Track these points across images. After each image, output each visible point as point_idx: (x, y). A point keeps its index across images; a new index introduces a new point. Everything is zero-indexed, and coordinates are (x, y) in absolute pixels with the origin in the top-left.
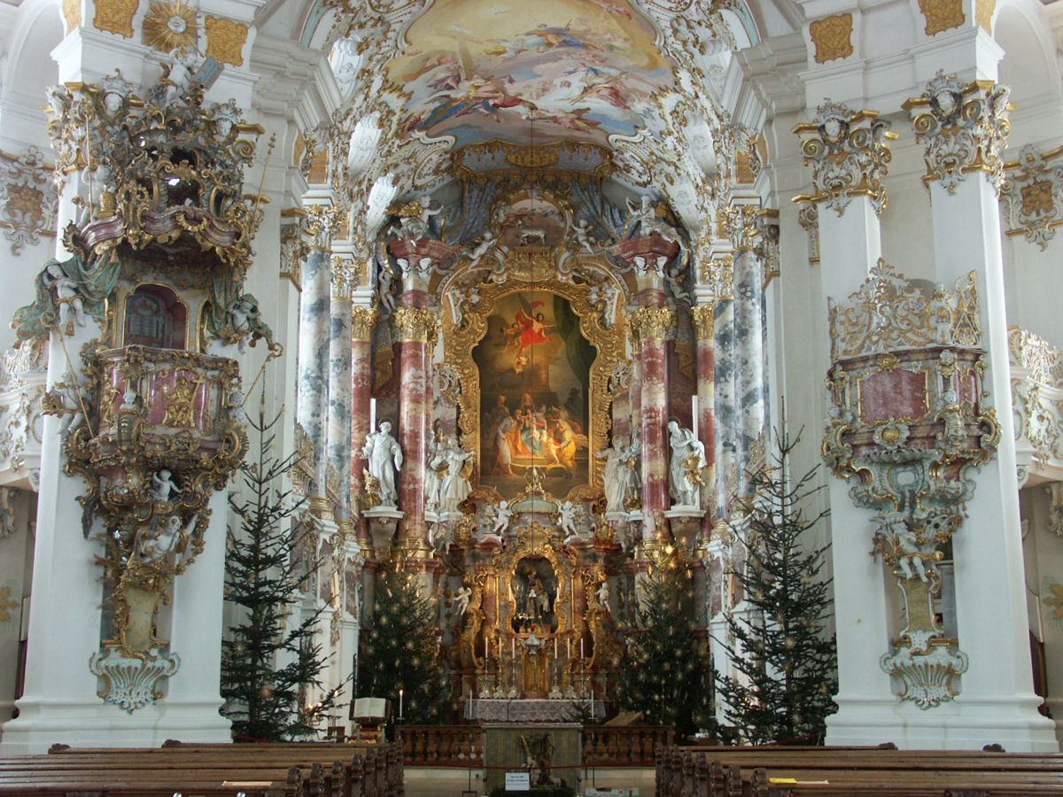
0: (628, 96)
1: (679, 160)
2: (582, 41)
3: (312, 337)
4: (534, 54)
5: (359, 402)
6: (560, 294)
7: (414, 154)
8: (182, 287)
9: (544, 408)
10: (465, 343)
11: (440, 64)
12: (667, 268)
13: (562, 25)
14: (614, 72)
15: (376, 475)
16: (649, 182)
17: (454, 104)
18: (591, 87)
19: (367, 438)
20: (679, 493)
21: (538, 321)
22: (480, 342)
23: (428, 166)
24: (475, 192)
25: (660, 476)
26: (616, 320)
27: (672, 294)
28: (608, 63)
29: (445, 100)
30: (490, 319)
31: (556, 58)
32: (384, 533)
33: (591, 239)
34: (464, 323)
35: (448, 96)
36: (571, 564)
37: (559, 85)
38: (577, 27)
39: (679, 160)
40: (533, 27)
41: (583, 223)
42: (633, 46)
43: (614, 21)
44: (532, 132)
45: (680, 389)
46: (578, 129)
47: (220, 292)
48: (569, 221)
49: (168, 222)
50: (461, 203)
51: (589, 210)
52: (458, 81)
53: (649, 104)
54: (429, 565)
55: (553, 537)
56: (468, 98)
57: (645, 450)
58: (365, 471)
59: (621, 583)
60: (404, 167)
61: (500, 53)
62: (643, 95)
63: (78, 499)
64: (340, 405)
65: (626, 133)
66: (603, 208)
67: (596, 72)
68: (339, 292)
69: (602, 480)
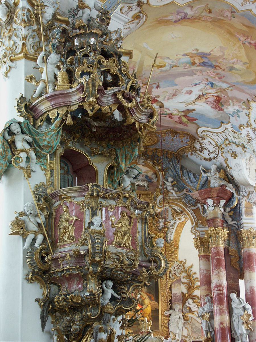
4: (181, 69)
8: (92, 153)
16: (214, 158)
18: (203, 95)
26: (174, 238)
31: (192, 74)
33: (175, 189)
37: (185, 92)
41: (170, 179)
42: (247, 68)
46: (181, 123)
47: (122, 159)
49: (110, 98)
51: (173, 173)
53: (240, 107)
57: (216, 308)
62: (239, 101)
63: (37, 300)
65: (212, 126)
66: (182, 172)
67: (212, 85)
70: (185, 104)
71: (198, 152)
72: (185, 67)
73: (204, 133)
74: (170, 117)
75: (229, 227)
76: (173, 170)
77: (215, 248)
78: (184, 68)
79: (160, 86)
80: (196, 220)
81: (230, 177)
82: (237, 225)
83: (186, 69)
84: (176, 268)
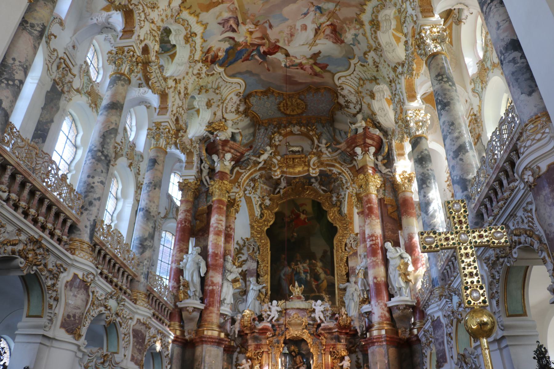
1: (377, 71)
3: (103, 124)
6: (316, 199)
7: (218, 88)
9: (308, 261)
10: (262, 226)
12: (376, 154)
15: (187, 279)
17: (239, 48)
19: (185, 257)
21: (303, 214)
22: (271, 226)
23: (230, 104)
24: (262, 131)
25: (382, 278)
26: (348, 211)
27: (380, 172)
30: (277, 214)
32: (191, 320)
34: (262, 215)
35: (233, 39)
36: (321, 344)
37: (300, 28)
39: (377, 71)
41: (324, 141)
44: (289, 80)
45: (389, 226)
46: (316, 74)
48: (316, 142)
50: (254, 134)
52: (238, 25)
54: (218, 342)
55: (309, 324)
56: (246, 43)
58: (181, 277)
59: (358, 359)
60: (211, 95)
68: (157, 144)
69: (344, 303)
70: (308, 46)
71: (346, 109)
73: (340, 81)
74: (302, 68)
75: (383, 175)
76: (328, 134)
77: (365, 196)
79: (272, 24)
84: (352, 241)
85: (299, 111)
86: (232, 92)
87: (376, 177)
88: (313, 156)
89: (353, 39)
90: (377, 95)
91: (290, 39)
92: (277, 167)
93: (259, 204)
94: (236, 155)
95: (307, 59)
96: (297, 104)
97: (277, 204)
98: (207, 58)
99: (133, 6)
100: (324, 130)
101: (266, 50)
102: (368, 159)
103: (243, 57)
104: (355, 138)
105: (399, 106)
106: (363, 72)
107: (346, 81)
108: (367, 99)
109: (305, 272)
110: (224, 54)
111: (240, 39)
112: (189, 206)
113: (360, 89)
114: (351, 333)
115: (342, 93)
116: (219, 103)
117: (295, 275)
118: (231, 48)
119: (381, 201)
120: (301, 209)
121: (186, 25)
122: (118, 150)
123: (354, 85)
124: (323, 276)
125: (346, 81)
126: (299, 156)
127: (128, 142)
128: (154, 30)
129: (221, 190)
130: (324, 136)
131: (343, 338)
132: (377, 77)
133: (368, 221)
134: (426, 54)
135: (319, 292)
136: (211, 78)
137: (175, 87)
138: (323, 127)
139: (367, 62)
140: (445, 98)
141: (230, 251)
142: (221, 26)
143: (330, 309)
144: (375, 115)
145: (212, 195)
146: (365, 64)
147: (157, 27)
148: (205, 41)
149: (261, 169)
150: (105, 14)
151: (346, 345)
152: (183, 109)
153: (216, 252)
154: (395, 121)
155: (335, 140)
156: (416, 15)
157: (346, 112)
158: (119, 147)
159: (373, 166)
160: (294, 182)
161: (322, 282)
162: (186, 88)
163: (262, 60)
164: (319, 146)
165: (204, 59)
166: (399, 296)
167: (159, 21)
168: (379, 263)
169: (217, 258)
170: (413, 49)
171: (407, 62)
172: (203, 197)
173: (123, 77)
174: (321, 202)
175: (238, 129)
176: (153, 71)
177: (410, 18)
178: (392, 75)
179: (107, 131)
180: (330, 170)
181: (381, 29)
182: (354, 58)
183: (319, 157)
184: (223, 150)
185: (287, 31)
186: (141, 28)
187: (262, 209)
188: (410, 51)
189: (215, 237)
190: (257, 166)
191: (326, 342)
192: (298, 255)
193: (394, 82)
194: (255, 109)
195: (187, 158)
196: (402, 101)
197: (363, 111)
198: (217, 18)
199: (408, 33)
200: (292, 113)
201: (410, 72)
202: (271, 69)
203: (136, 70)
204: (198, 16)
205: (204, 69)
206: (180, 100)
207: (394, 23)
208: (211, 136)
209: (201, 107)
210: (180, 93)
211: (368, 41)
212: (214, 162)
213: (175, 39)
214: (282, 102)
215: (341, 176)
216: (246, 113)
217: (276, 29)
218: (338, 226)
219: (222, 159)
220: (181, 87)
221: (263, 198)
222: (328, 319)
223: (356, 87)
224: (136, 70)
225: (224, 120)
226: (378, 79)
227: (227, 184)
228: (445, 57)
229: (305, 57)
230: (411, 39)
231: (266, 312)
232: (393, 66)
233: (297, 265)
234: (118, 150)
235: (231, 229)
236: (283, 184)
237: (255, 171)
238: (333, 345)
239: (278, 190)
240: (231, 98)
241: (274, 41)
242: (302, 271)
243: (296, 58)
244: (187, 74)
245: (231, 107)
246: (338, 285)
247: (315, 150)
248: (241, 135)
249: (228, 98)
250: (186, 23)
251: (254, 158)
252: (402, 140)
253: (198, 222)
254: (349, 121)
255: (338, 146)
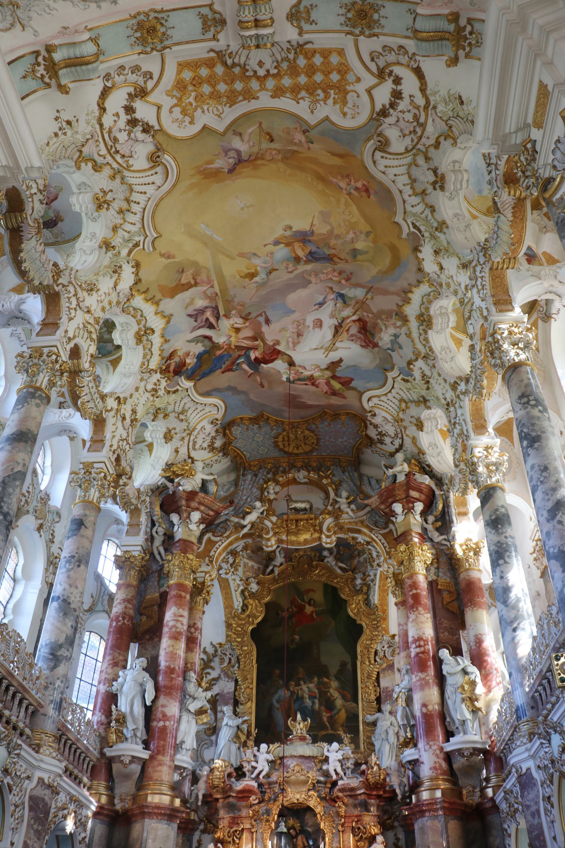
0: (375, 325)
1: (428, 389)
2: (327, 252)
5: (117, 639)
6: (329, 583)
9: (316, 679)
11: (196, 284)
12: (424, 514)
13: (307, 228)
14: (359, 293)
16: (401, 446)
17: (218, 353)
20: (457, 722)
21: (310, 605)
24: (249, 477)
26: (379, 600)
28: (353, 281)
29: (207, 342)
30: (267, 605)
34: (245, 607)
35: (209, 338)
36: (338, 814)
37: (311, 325)
38: (322, 229)
39: (428, 389)
40: (279, 232)
41: (344, 494)
43: (354, 208)
46: (334, 393)
48: (332, 495)
50: (236, 483)
51: (349, 486)
52: (218, 318)
61: (252, 276)
64: (64, 601)
68: (85, 496)
69: (373, 745)
70: (323, 351)
71: (379, 445)
72: (290, 270)
73: (371, 404)
74: (313, 384)
78: (289, 272)
80: (387, 549)
81: (427, 468)
82: (449, 541)
83: (291, 272)
84: (386, 646)
85: (307, 448)
86: (204, 418)
87: (425, 548)
88: (327, 516)
89: (391, 341)
90: (427, 425)
91: (296, 341)
92: (271, 533)
93: (240, 590)
94: (208, 515)
95: (321, 370)
96: (304, 437)
97: (270, 591)
98: (168, 367)
99: (61, 286)
100: (345, 477)
101: (260, 357)
102: (412, 520)
103: (224, 366)
104: (393, 489)
105: (460, 441)
106: (405, 390)
107: (380, 403)
108: (412, 430)
109: (312, 697)
110: (195, 360)
111: (220, 339)
112: (132, 592)
113: (401, 415)
114: (386, 795)
115: (373, 421)
116: (184, 435)
117: (295, 701)
118: (205, 352)
119: (432, 585)
120: (306, 598)
121: (139, 317)
122: (22, 503)
123: (392, 410)
124: (339, 702)
125: (380, 403)
126: (306, 516)
127: (37, 492)
128: (89, 323)
129: (183, 569)
130: (345, 485)
131: (373, 805)
132: (428, 398)
133: (412, 616)
134: (502, 365)
135: (332, 729)
136: (173, 397)
137: (117, 410)
138: (343, 472)
139: (412, 376)
140: (533, 430)
141: (193, 664)
142: (193, 320)
143: (352, 756)
144: (423, 454)
145: (168, 576)
146: (409, 378)
147: (95, 318)
148: (166, 341)
149: (244, 536)
150: (16, 297)
151: (378, 816)
152: (128, 443)
153: (172, 666)
154: (454, 463)
155: (362, 492)
156: (486, 308)
157: (378, 450)
158: (24, 499)
159: (420, 531)
160: (295, 556)
161: (338, 713)
162: (134, 412)
163: (252, 371)
164: (337, 502)
165: (164, 367)
166: (461, 734)
167: (99, 310)
168: (431, 681)
169: (173, 676)
170: (482, 357)
171: (474, 377)
172: (154, 579)
173: (39, 393)
174: (338, 586)
175: (212, 474)
176: (85, 384)
177: (478, 312)
178: (450, 395)
179: (9, 476)
180: (353, 538)
181: (434, 327)
182: (392, 369)
183: (337, 518)
184: (188, 506)
185: (292, 328)
186: (70, 319)
187: (245, 598)
188: (478, 360)
189: (170, 642)
190: (240, 532)
191: (345, 811)
192: (301, 670)
193: (453, 405)
194: (238, 444)
195: (131, 518)
196: (465, 433)
197: (404, 448)
198: (186, 308)
199: (474, 333)
200: (295, 451)
201: (479, 391)
202: (266, 384)
203: (59, 383)
204: (157, 303)
205: (164, 383)
206: (124, 429)
207: (453, 319)
208: (169, 485)
209: (155, 440)
210: (124, 418)
211: (414, 344)
212: (172, 524)
213: (120, 337)
214: (281, 434)
215: (369, 547)
216: (224, 450)
217: (275, 326)
218: (364, 624)
219: (186, 520)
220: (127, 409)
221: (247, 581)
222: (349, 772)
223: (394, 412)
224: (59, 383)
225: (190, 461)
226: (429, 400)
227: (192, 560)
228: (532, 370)
229: (318, 366)
230: (479, 343)
231: (249, 762)
232: (452, 381)
233: (299, 685)
234: (22, 503)
235: (196, 629)
236: (279, 559)
237: (237, 539)
238: (357, 816)
239: (271, 568)
240: (203, 428)
241: (272, 344)
242: (306, 696)
243: (305, 368)
244: (137, 389)
245: (202, 440)
246: (364, 716)
247: (330, 508)
248: (217, 484)
249: (199, 427)
250: (140, 313)
251: (236, 520)
252: (465, 492)
253: (144, 618)
254: (383, 463)
255: (366, 502)
